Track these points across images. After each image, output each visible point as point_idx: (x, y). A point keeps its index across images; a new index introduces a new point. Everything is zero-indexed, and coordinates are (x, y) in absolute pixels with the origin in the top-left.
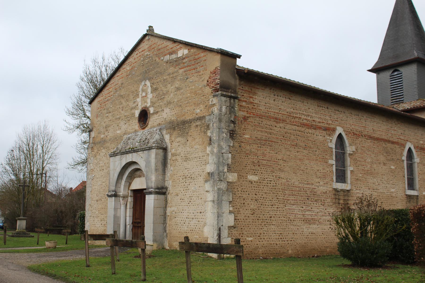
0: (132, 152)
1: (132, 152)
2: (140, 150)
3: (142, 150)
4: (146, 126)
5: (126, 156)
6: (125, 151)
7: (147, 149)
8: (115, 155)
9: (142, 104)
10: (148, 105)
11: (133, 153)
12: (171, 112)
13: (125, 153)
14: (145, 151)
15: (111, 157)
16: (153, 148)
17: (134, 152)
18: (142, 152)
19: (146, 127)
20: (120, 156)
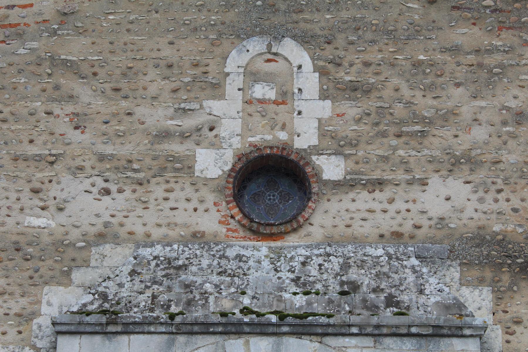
0: (285, 329)
1: (285, 329)
2: (355, 330)
3: (369, 330)
4: (295, 230)
5: (247, 343)
6: (217, 319)
7: (414, 330)
8: (111, 328)
9: (247, 129)
10: (300, 143)
11: (292, 342)
12: (481, 200)
13: (220, 329)
14: (388, 341)
15: (59, 333)
16: (467, 332)
17: (299, 334)
18: (368, 342)
19: (287, 233)
20: (166, 337)
